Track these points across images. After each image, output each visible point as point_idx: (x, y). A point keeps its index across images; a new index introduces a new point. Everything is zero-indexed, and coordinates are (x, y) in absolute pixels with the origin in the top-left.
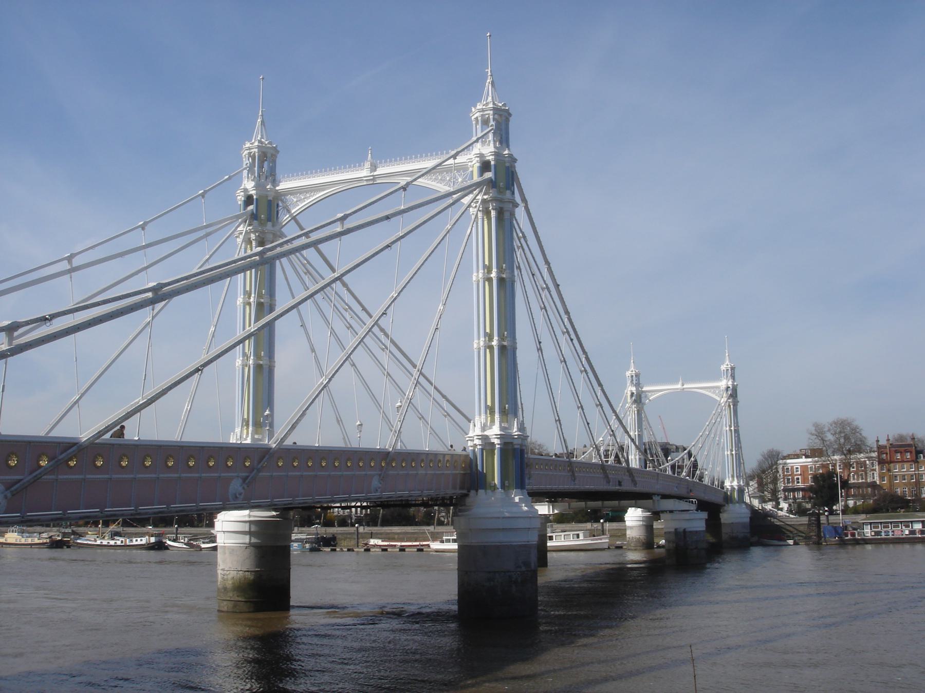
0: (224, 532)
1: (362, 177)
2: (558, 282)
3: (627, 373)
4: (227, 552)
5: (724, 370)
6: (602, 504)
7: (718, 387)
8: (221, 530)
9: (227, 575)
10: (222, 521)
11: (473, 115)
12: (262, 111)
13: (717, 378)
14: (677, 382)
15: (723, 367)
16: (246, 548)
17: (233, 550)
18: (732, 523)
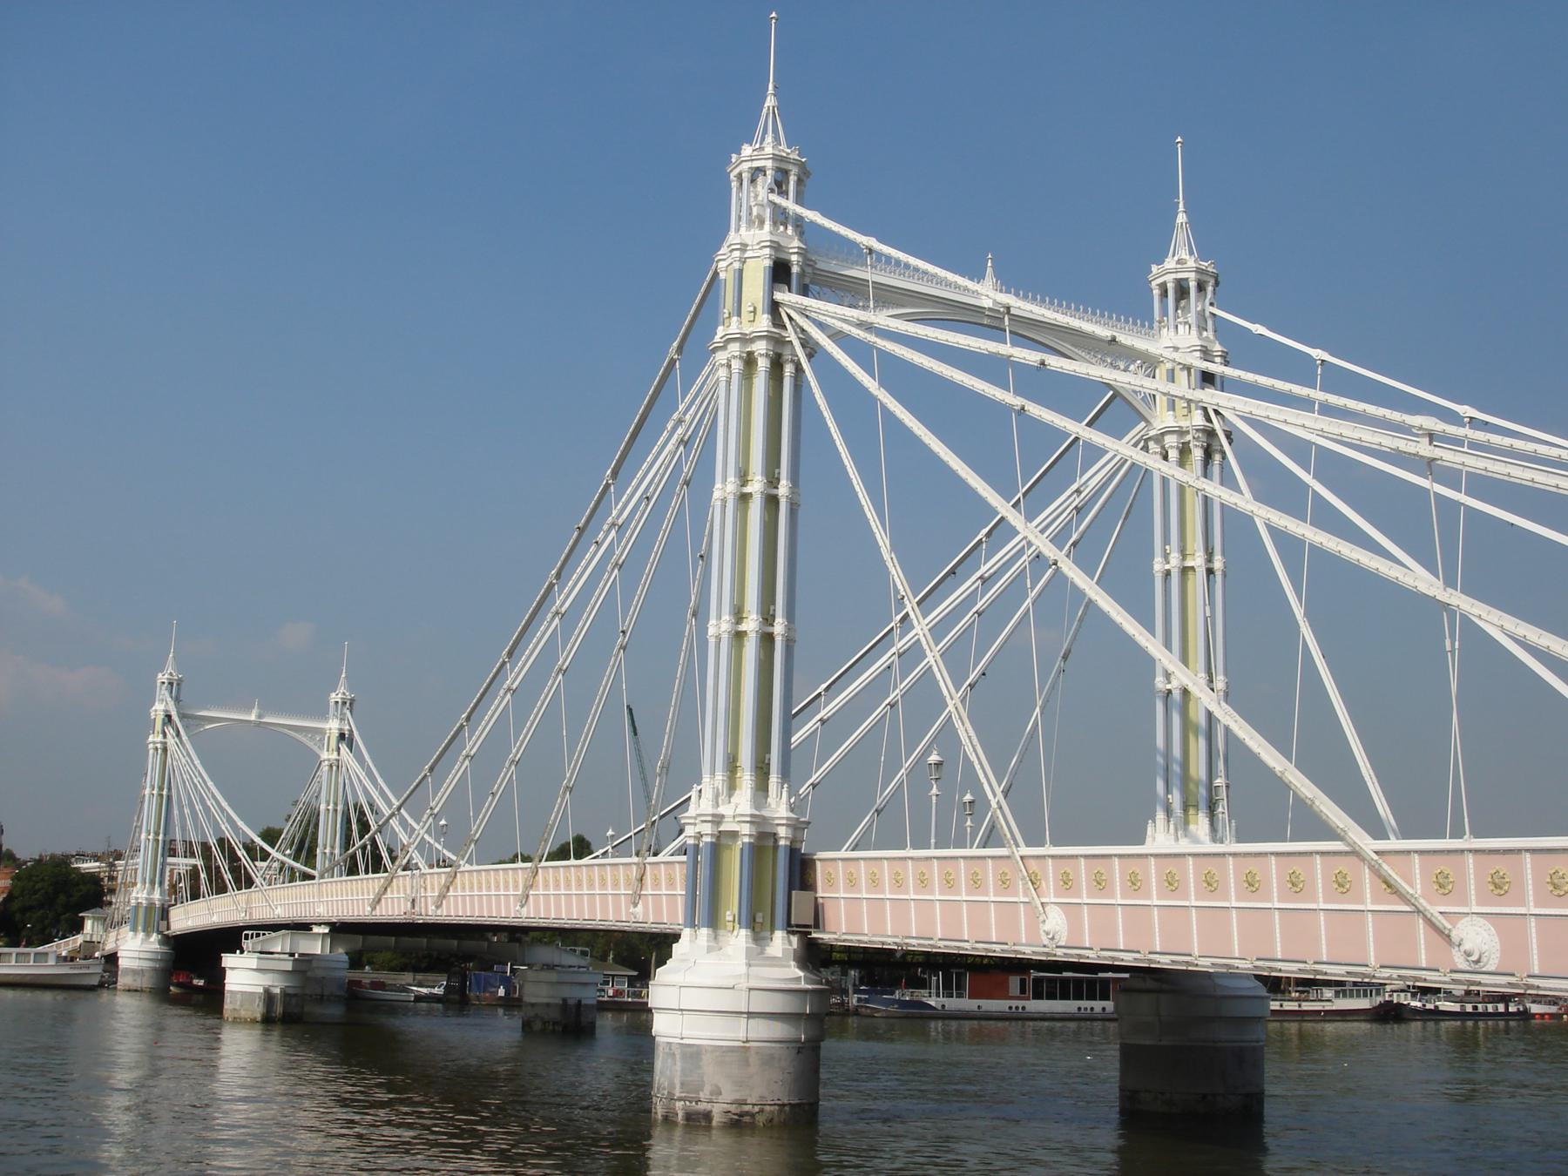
0: (682, 1010)
1: (985, 308)
2: (959, 568)
3: (160, 675)
4: (753, 1059)
5: (337, 702)
6: (396, 942)
7: (321, 732)
8: (677, 1008)
9: (752, 1115)
10: (750, 989)
11: (1177, 272)
12: (775, 87)
13: (323, 714)
14: (249, 709)
15: (335, 697)
16: (799, 1052)
17: (772, 1057)
18: (323, 978)
